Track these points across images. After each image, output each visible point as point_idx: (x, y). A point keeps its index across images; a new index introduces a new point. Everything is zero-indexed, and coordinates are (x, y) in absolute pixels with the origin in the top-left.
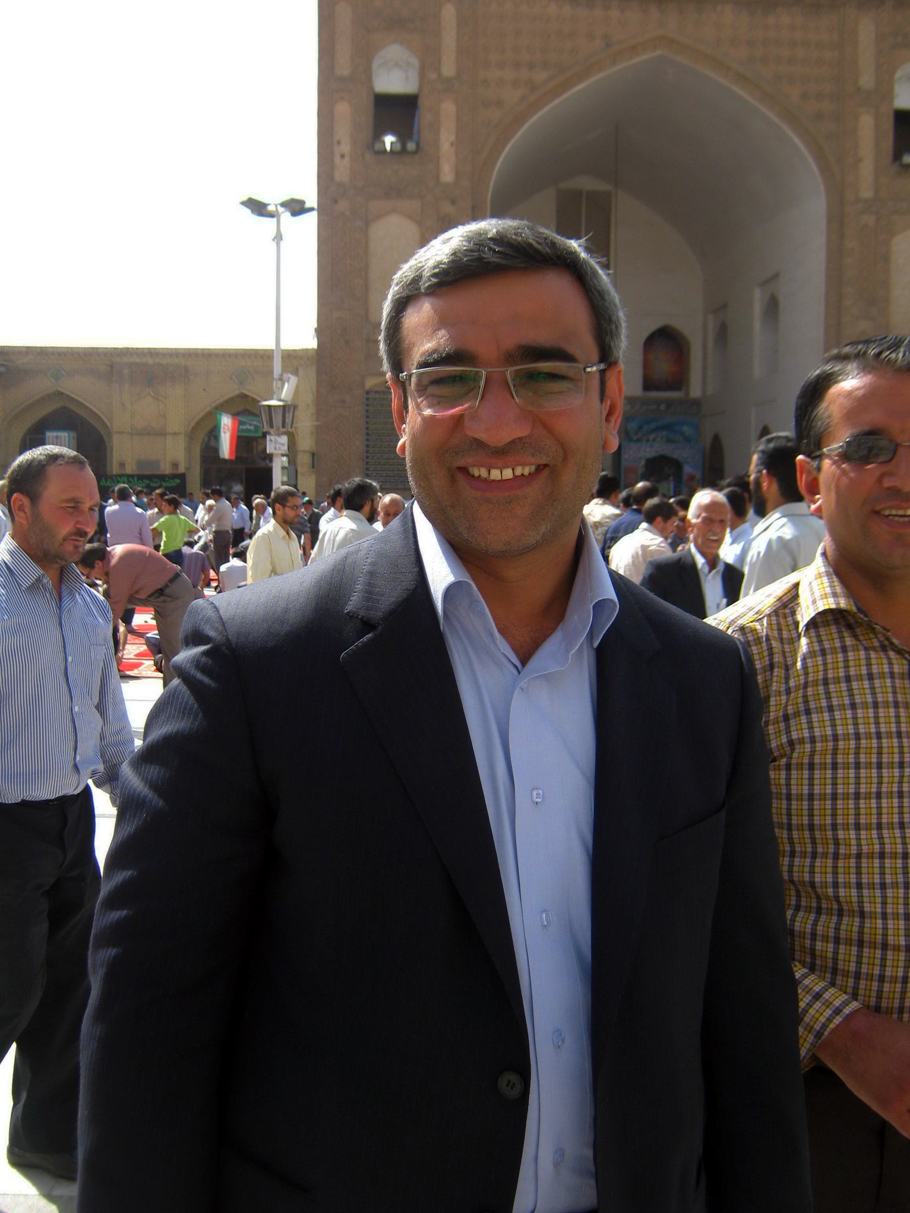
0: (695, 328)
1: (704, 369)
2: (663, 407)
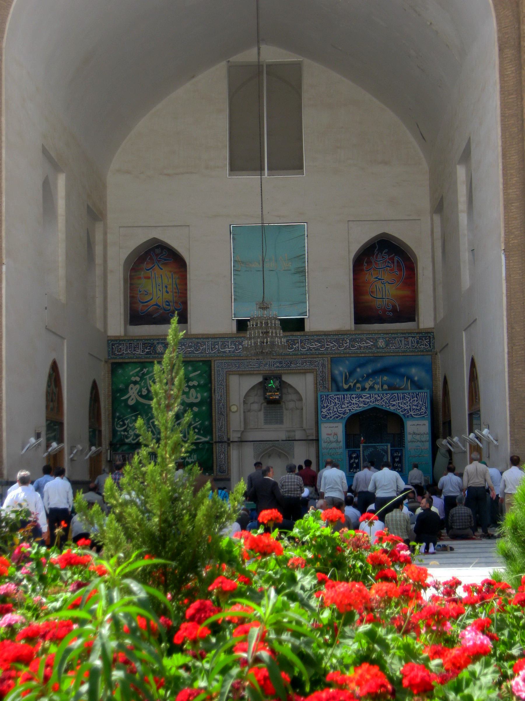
0: (418, 237)
1: (434, 289)
2: (381, 343)
